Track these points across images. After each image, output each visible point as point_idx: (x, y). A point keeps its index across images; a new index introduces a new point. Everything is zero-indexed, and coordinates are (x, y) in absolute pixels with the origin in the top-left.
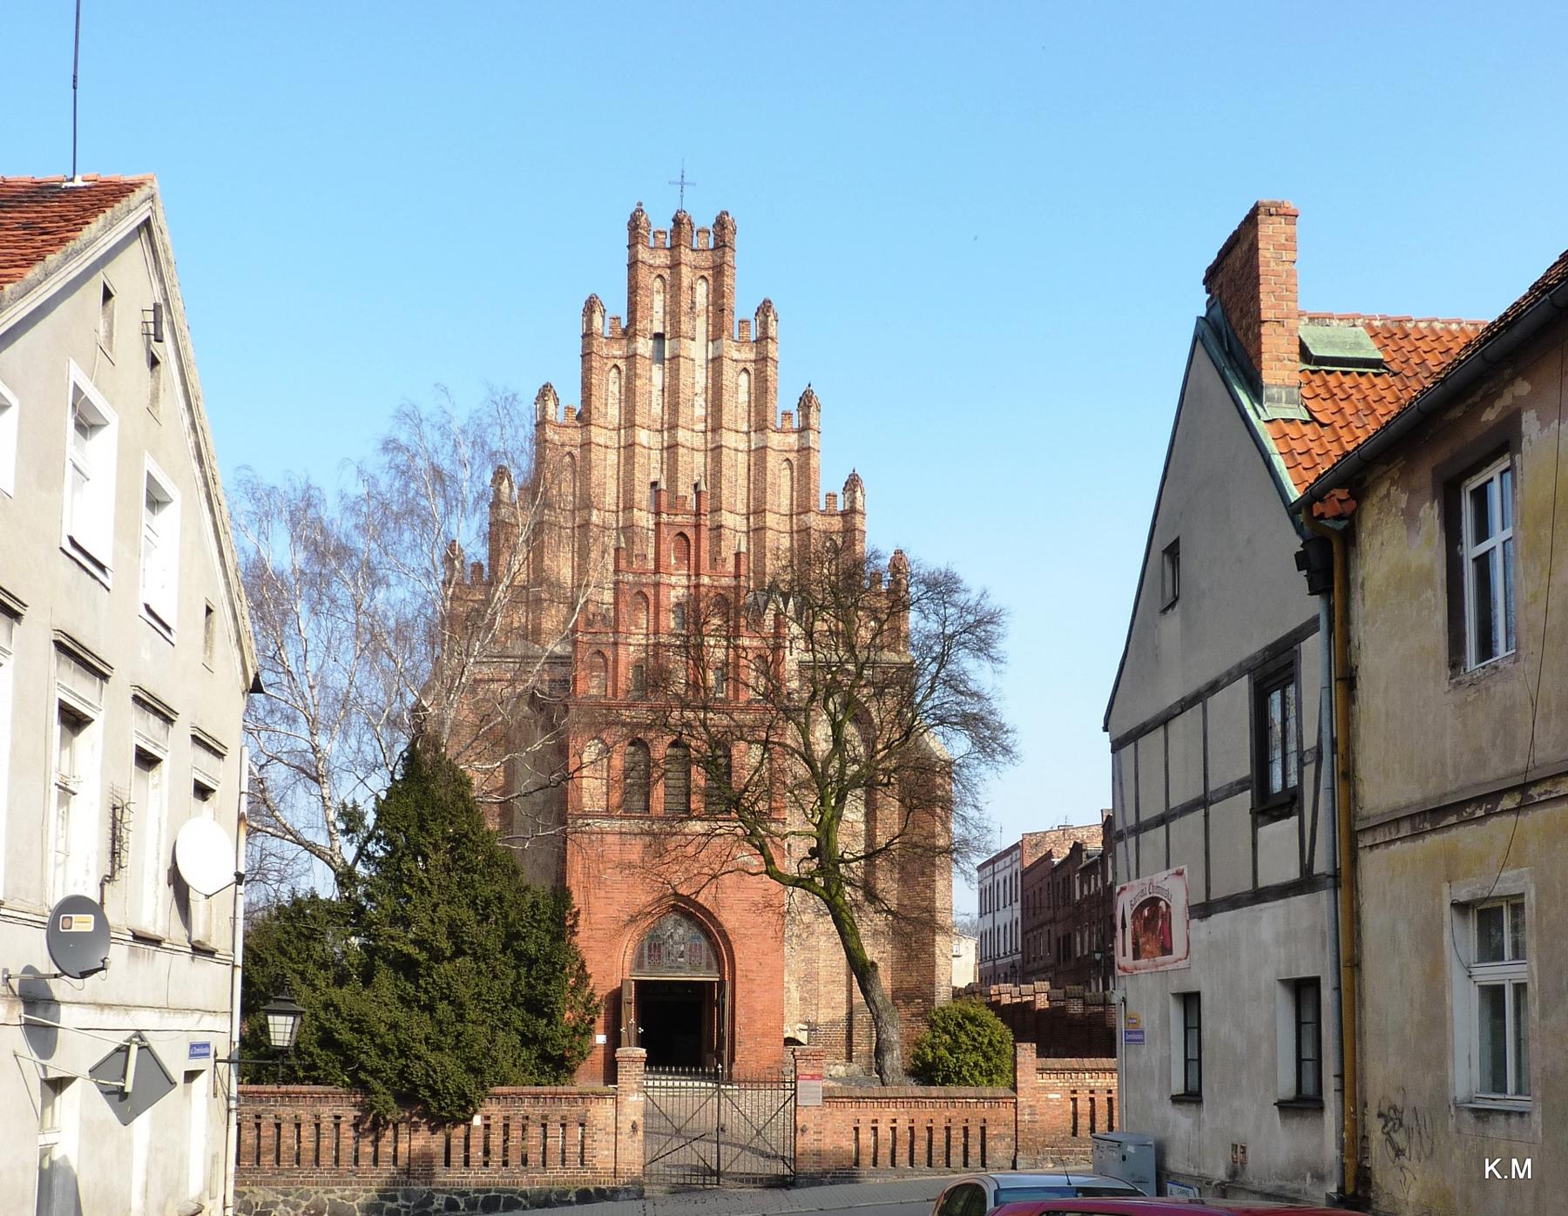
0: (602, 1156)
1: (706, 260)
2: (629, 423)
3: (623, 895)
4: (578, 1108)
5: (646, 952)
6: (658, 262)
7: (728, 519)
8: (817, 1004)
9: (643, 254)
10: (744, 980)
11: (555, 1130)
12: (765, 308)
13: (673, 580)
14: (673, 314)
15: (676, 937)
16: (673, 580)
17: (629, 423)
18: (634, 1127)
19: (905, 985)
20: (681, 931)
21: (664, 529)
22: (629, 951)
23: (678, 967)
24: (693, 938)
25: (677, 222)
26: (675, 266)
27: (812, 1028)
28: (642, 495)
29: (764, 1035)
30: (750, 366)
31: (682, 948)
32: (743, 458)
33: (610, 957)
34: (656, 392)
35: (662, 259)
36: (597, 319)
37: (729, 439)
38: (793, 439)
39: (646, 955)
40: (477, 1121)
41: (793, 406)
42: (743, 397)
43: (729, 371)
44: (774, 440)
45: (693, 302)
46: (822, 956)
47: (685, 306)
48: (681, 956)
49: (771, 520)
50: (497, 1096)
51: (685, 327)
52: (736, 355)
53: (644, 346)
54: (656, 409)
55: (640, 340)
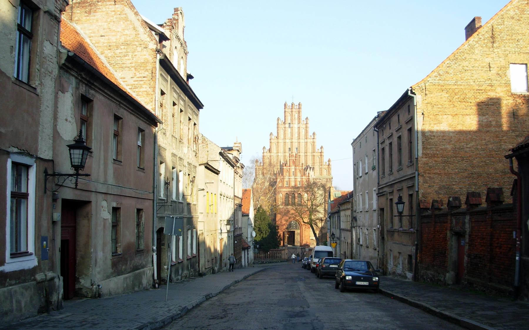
0: (283, 257)
1: (297, 110)
2: (285, 138)
6: (289, 111)
7: (301, 154)
9: (287, 110)
11: (277, 254)
12: (307, 118)
13: (292, 168)
14: (292, 120)
16: (292, 168)
17: (285, 138)
21: (290, 160)
25: (292, 104)
26: (292, 112)
28: (287, 150)
30: (305, 128)
32: (304, 143)
34: (289, 133)
35: (290, 110)
36: (279, 121)
37: (301, 141)
38: (312, 140)
40: (269, 253)
41: (312, 135)
42: (303, 133)
43: (301, 129)
44: (309, 141)
47: (294, 119)
49: (308, 154)
50: (271, 250)
51: (294, 122)
52: (302, 126)
53: (287, 125)
54: (289, 136)
55: (286, 124)
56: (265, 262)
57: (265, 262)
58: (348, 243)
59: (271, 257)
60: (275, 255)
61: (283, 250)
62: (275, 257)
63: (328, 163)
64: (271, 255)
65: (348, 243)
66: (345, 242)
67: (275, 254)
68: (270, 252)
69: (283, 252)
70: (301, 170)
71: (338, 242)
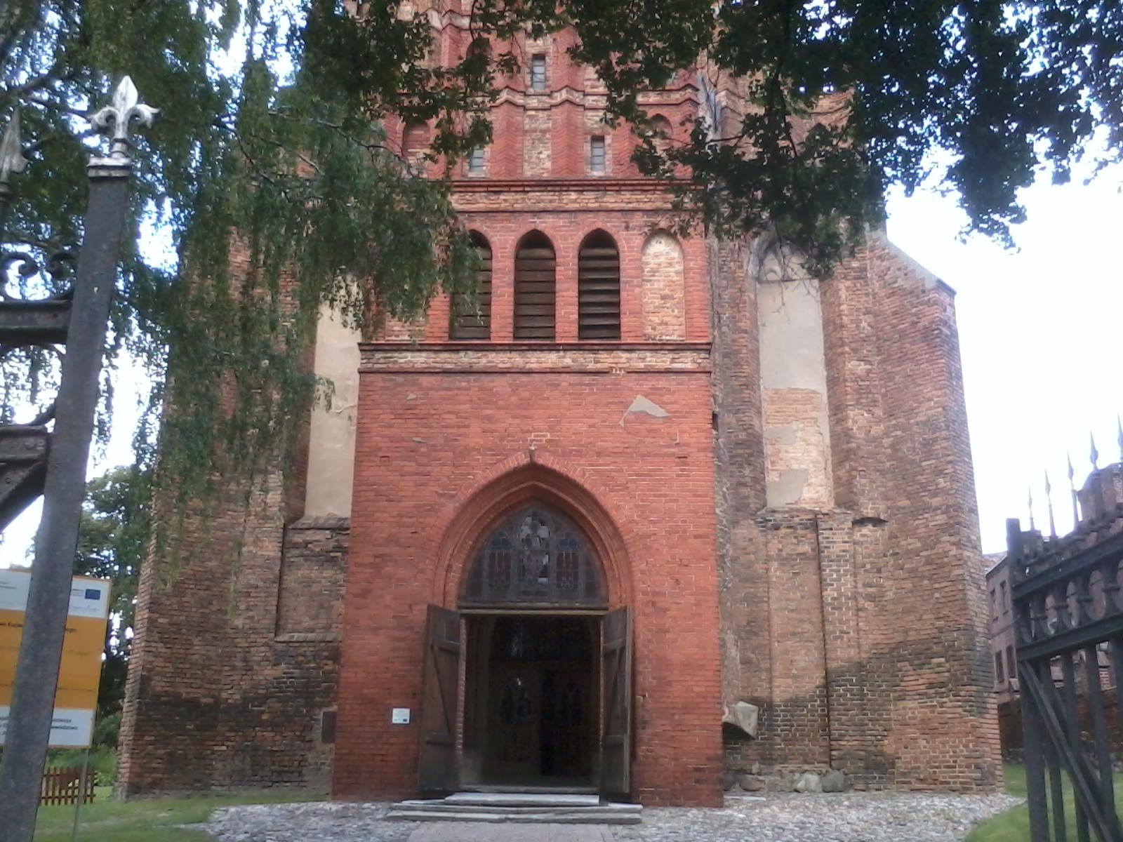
3: (447, 469)
5: (486, 567)
8: (770, 670)
10: (649, 609)
15: (536, 543)
19: (912, 636)
20: (544, 532)
22: (458, 565)
23: (538, 593)
24: (563, 543)
27: (765, 707)
29: (687, 709)
31: (545, 560)
33: (422, 571)
39: (485, 574)
46: (774, 594)
48: (545, 572)
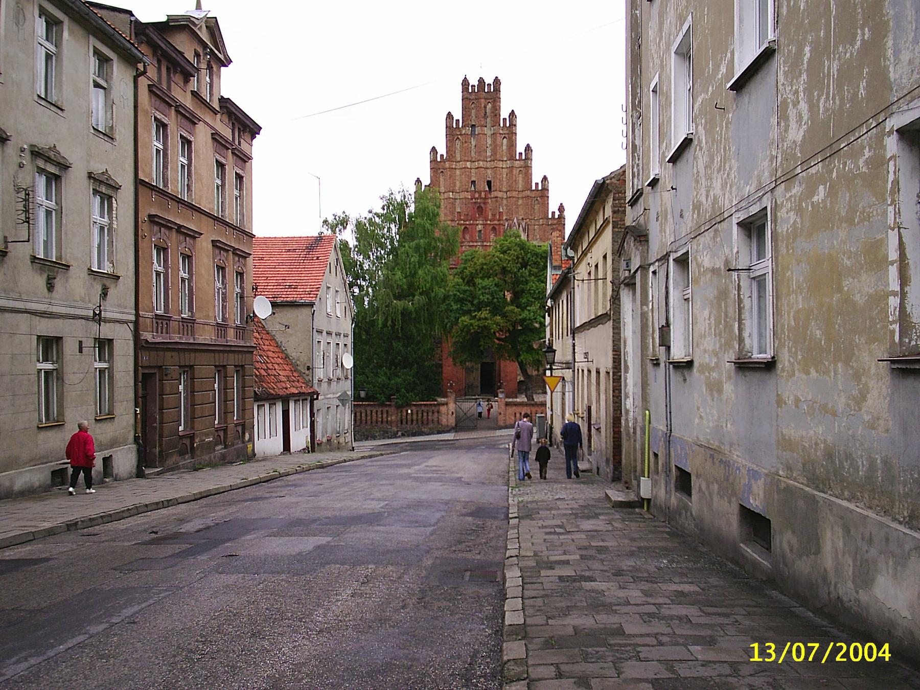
0: (444, 421)
4: (437, 408)
11: (430, 414)
12: (512, 114)
18: (453, 413)
42: (504, 148)
45: (486, 112)
52: (501, 132)
56: (400, 434)
57: (400, 434)
58: (598, 372)
59: (415, 422)
60: (425, 417)
61: (443, 405)
62: (425, 422)
63: (557, 214)
64: (415, 417)
65: (598, 372)
66: (589, 371)
67: (425, 414)
68: (414, 408)
69: (443, 409)
70: (497, 227)
71: (568, 374)
